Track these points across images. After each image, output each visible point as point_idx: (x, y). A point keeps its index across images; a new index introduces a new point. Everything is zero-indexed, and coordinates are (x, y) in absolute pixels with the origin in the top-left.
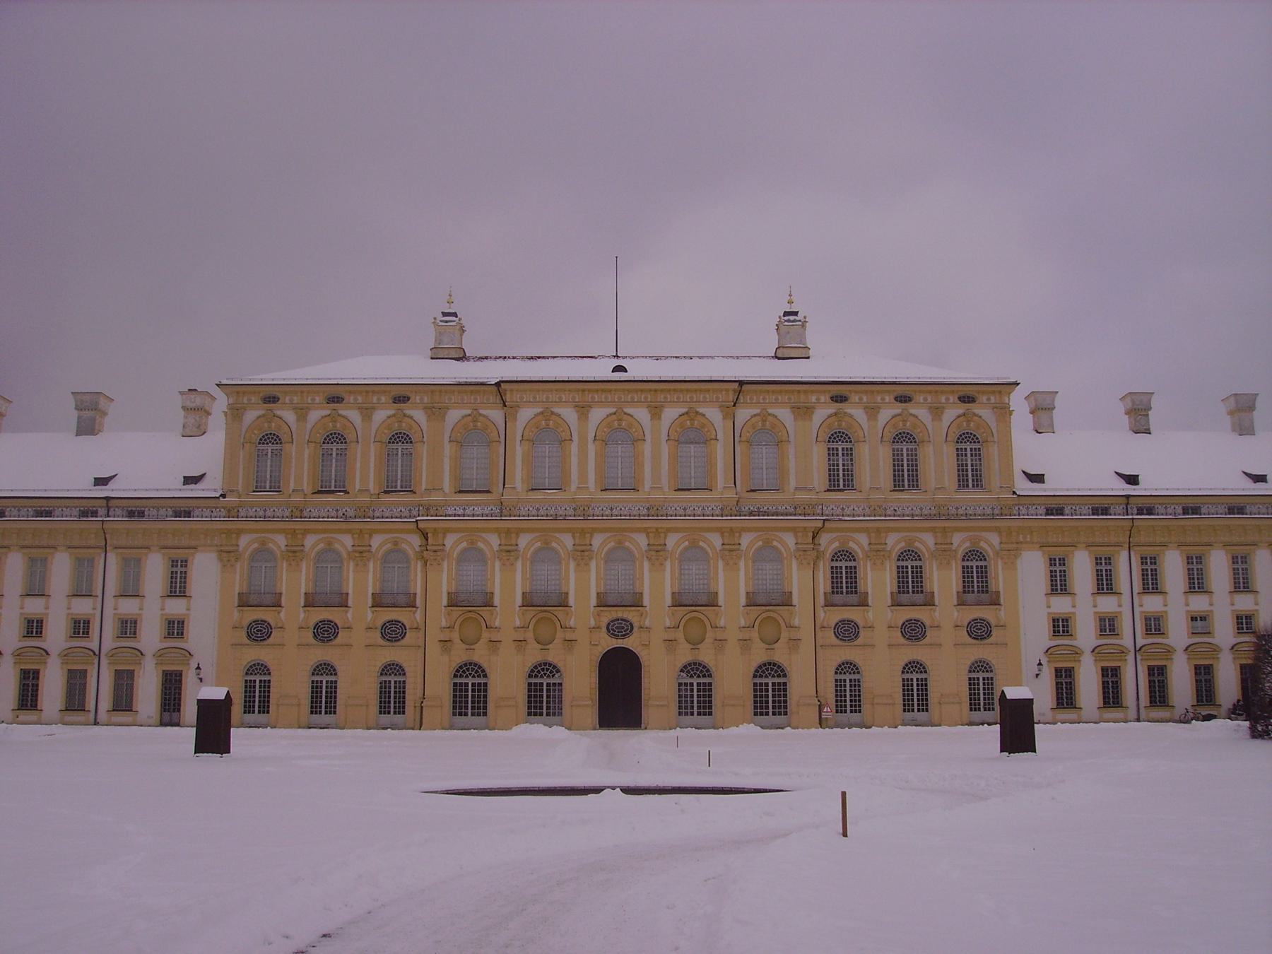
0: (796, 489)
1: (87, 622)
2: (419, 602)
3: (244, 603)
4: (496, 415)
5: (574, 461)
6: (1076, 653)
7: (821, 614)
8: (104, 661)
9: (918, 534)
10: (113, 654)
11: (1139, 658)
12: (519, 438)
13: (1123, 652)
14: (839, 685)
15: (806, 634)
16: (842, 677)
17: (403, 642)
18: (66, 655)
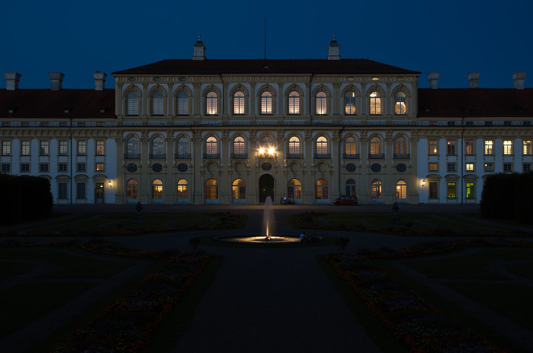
0: (334, 114)
1: (65, 165)
2: (192, 157)
3: (126, 157)
4: (220, 86)
5: (250, 103)
6: (439, 178)
7: (342, 162)
8: (73, 180)
9: (379, 132)
10: (76, 177)
11: (463, 180)
12: (229, 95)
13: (457, 178)
14: (348, 188)
15: (336, 169)
16: (349, 185)
17: (186, 172)
18: (57, 178)
